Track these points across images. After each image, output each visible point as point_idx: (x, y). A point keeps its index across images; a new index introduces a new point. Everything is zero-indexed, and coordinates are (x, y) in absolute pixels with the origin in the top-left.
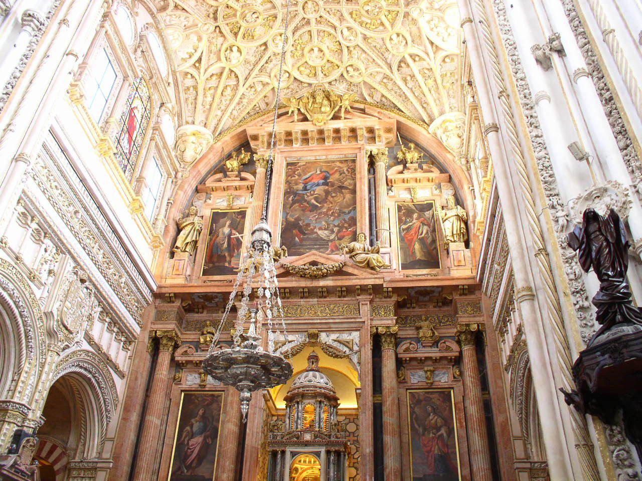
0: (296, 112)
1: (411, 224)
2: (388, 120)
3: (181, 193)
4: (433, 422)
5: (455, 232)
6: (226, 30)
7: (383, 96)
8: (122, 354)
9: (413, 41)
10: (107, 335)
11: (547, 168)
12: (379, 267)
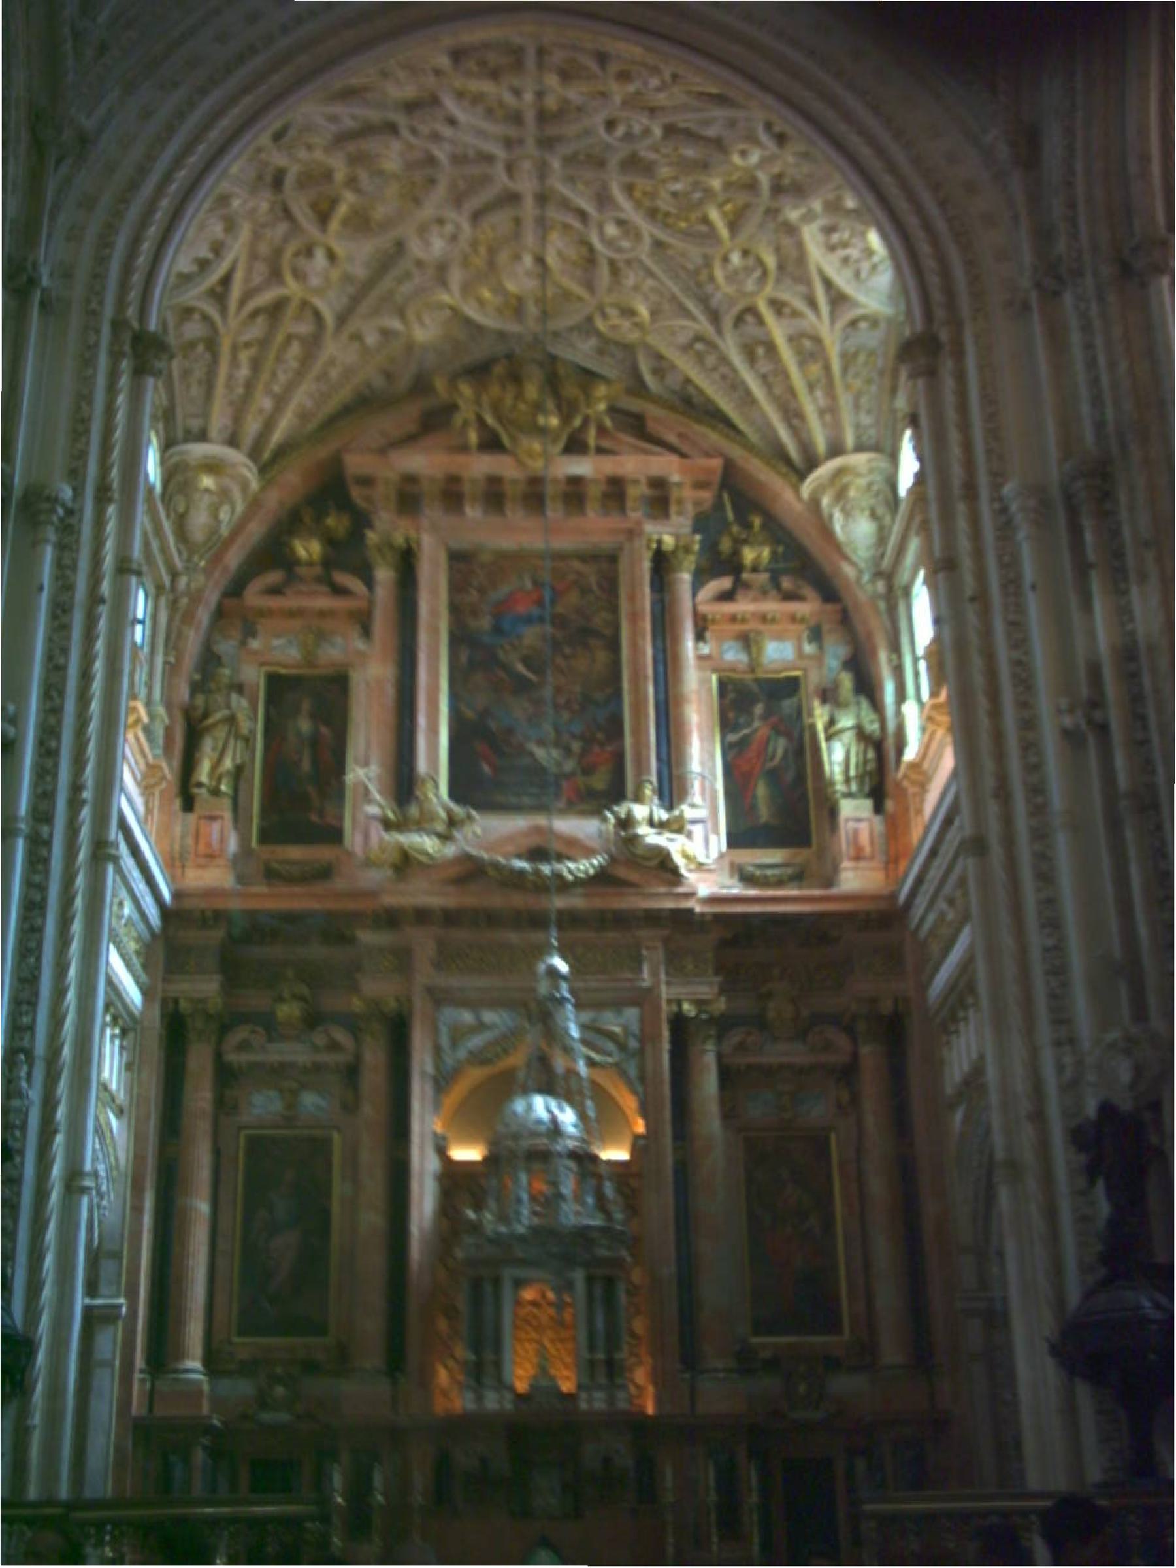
1: (746, 731)
2: (703, 462)
5: (852, 773)
9: (781, 267)
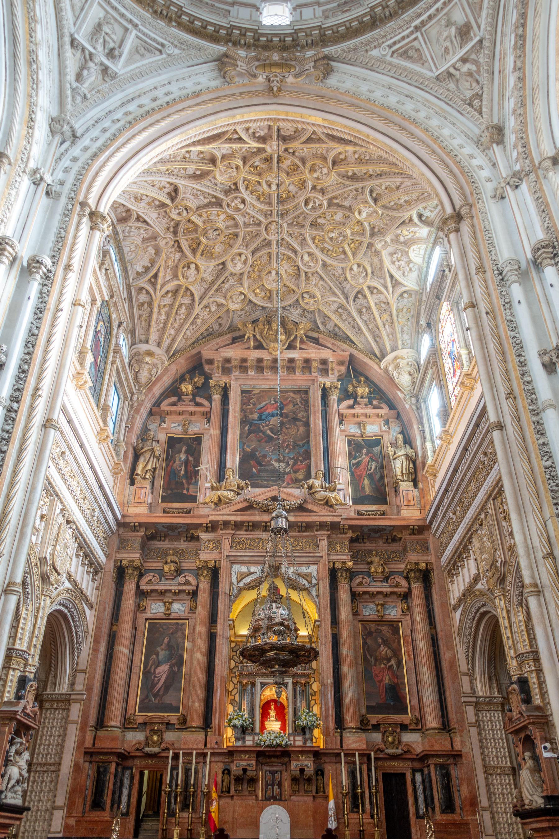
9: (373, 273)
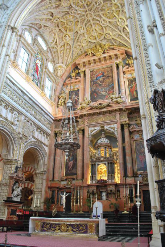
0: (91, 53)
2: (121, 50)
3: (58, 87)
4: (143, 150)
6: (63, 30)
7: (119, 42)
8: (46, 139)
10: (40, 135)
11: (150, 72)
12: (121, 102)
